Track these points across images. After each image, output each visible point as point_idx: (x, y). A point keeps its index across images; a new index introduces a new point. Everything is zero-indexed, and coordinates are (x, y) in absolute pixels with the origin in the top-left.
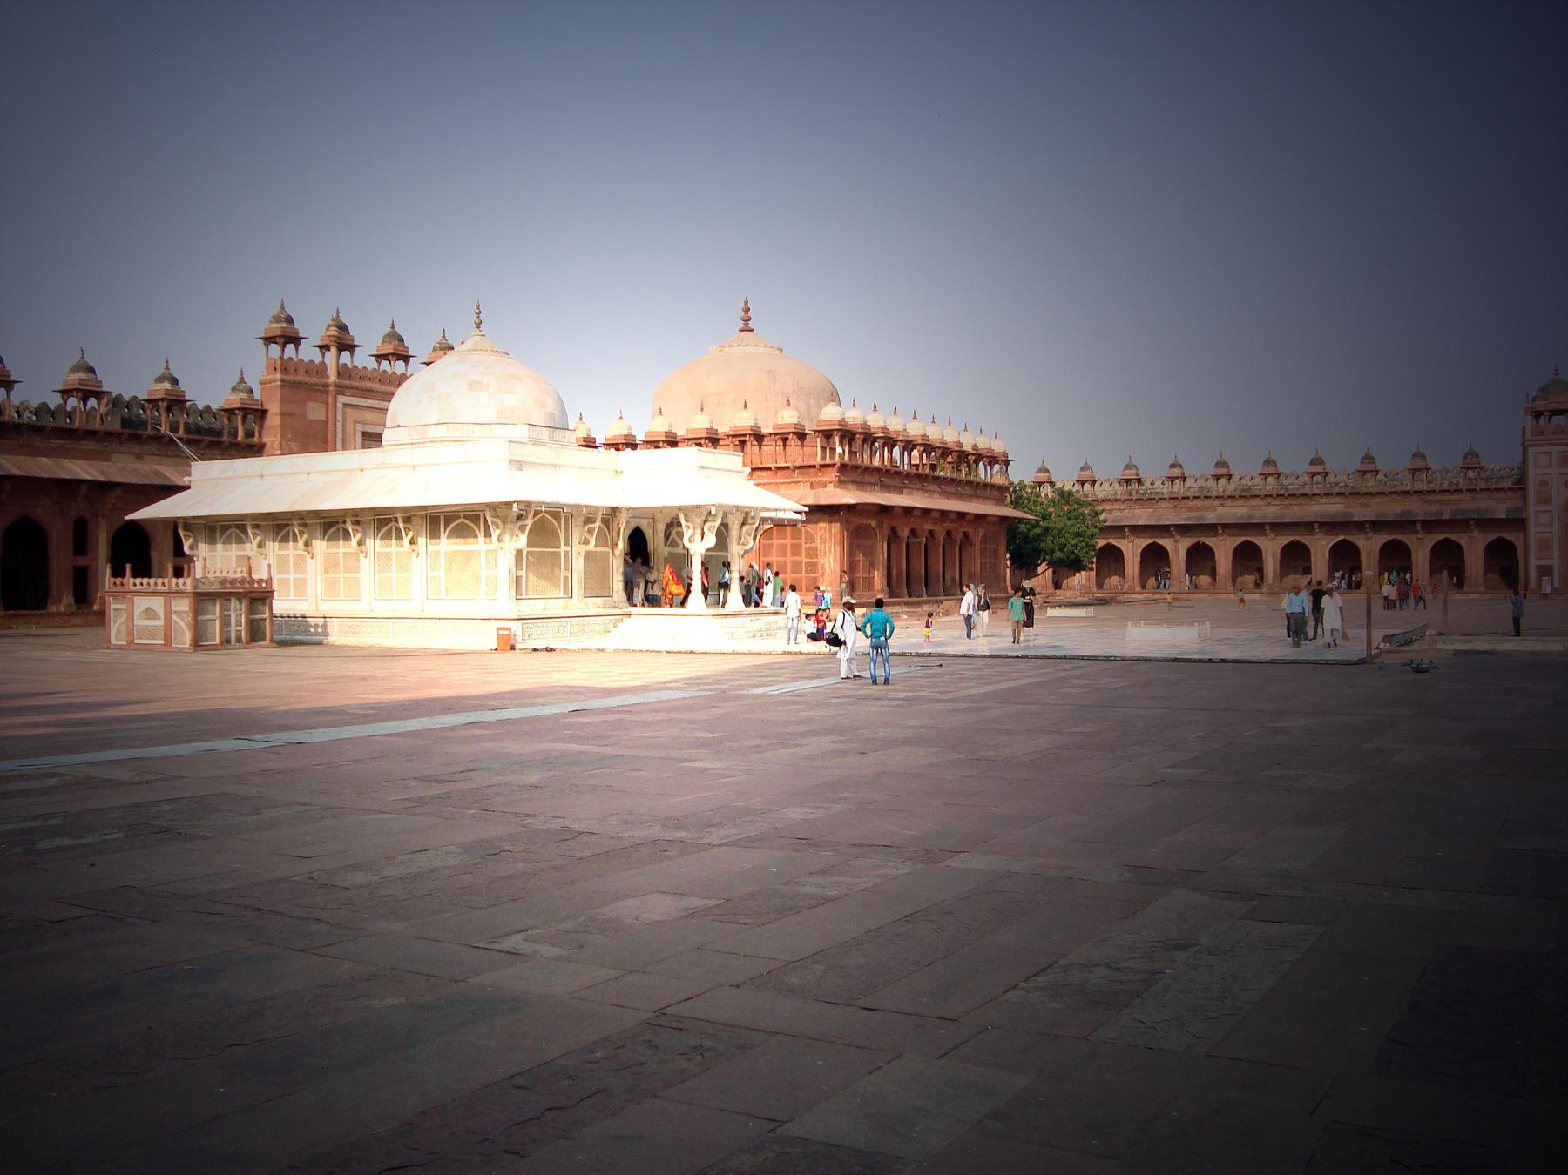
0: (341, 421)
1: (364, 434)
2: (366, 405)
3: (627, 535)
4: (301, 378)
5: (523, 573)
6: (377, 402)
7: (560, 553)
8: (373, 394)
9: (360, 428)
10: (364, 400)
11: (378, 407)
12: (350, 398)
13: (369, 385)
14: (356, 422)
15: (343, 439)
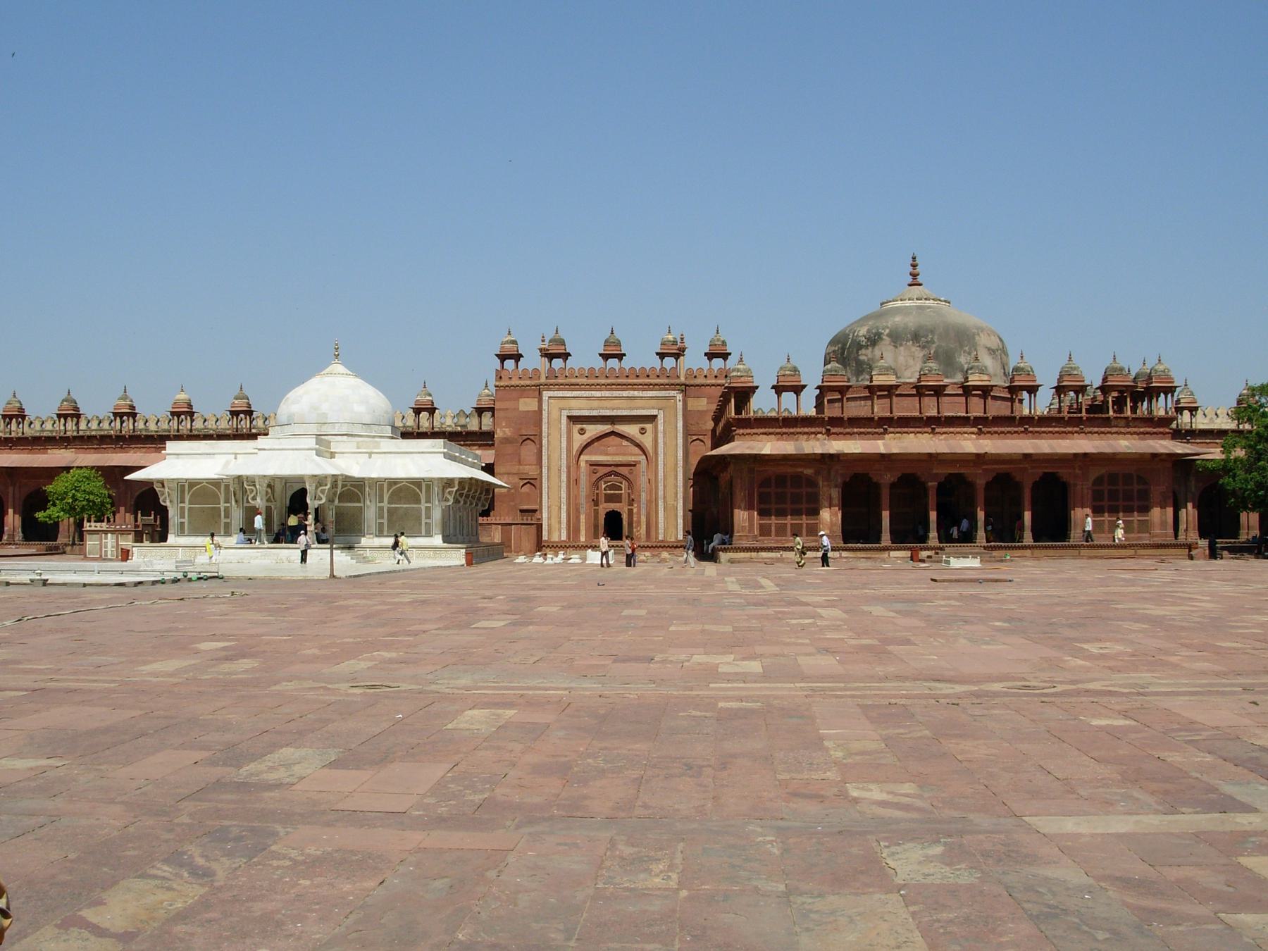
0: (547, 410)
1: (569, 417)
2: (573, 395)
3: (289, 494)
4: (515, 382)
5: (186, 520)
6: (583, 392)
7: (219, 508)
8: (578, 387)
9: (565, 413)
10: (570, 392)
11: (585, 396)
12: (556, 392)
13: (574, 381)
14: (561, 409)
15: (548, 422)
